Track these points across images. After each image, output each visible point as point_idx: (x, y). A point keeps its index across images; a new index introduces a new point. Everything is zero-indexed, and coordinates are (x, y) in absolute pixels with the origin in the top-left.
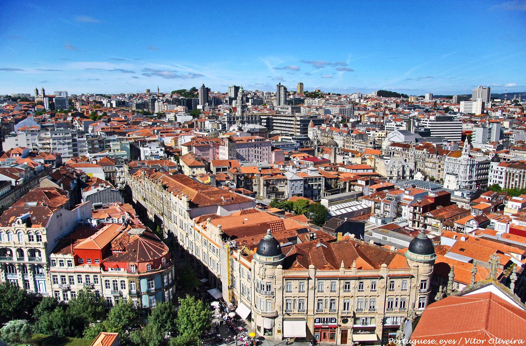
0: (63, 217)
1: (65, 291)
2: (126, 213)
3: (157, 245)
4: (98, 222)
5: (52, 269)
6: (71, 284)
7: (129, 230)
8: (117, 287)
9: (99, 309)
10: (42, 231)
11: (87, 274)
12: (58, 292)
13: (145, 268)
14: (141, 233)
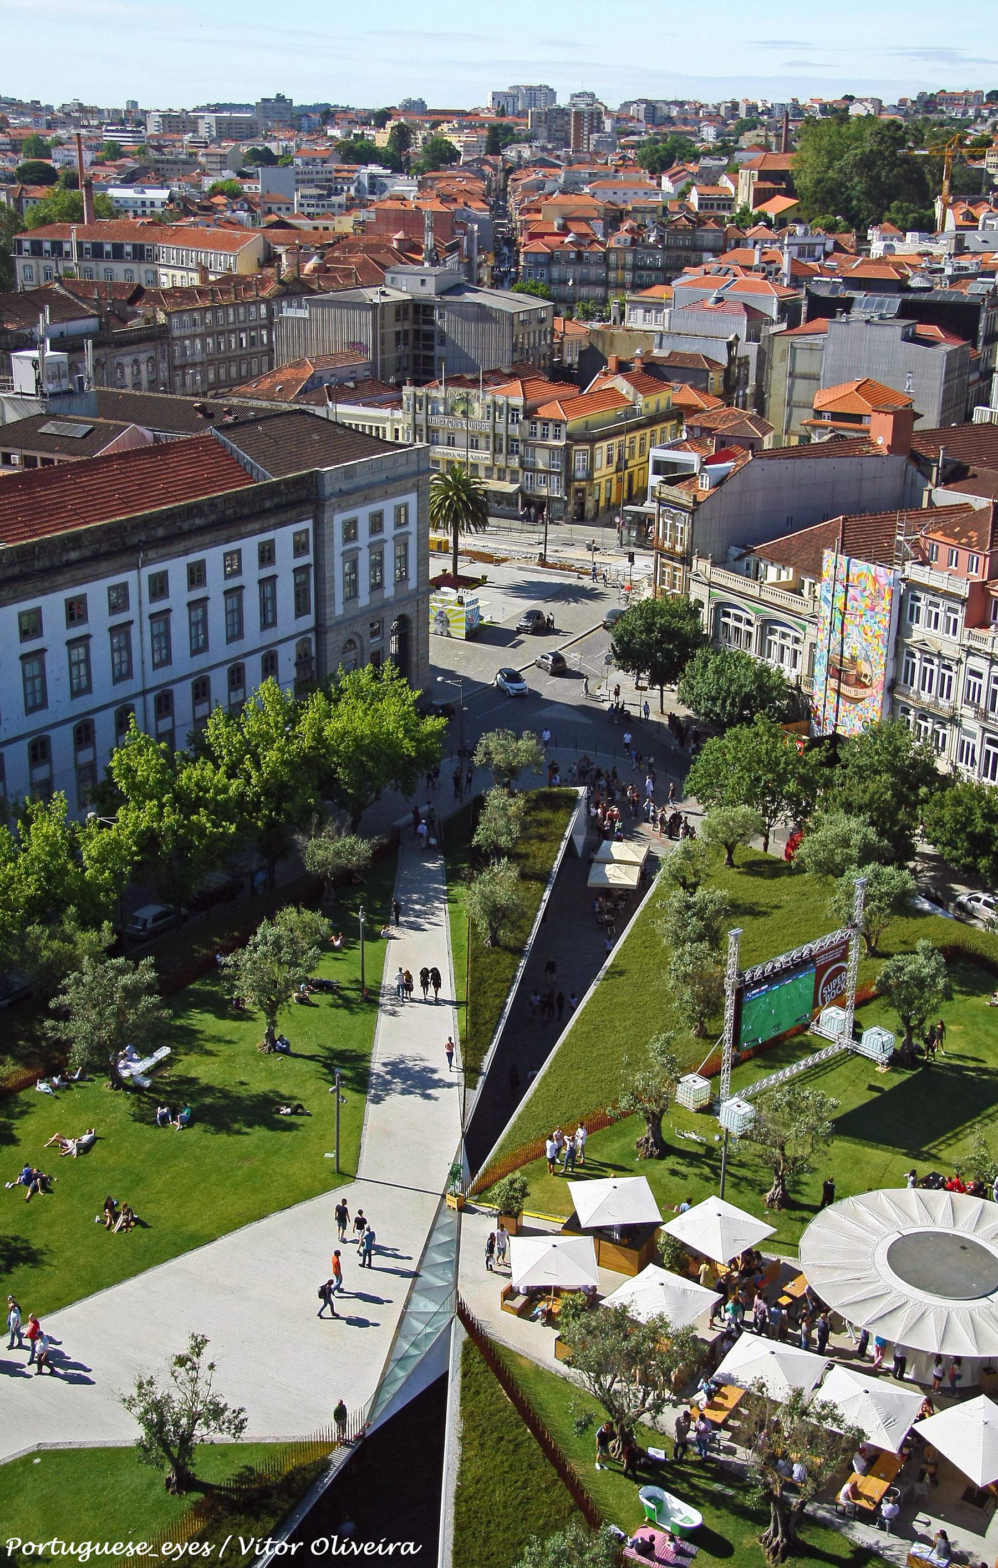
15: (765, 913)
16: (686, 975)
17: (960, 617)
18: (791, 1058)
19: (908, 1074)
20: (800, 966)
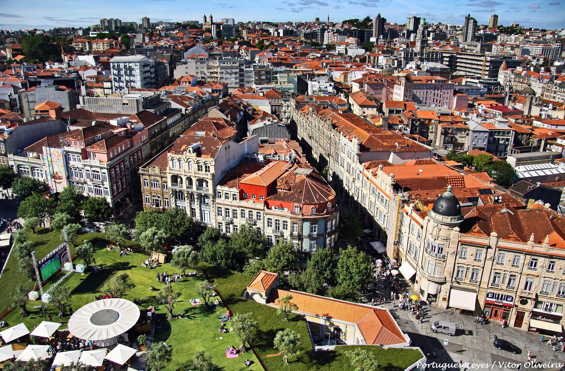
0: (231, 149)
2: (293, 151)
3: (323, 188)
4: (265, 158)
5: (218, 200)
7: (295, 169)
9: (260, 246)
10: (211, 161)
11: (250, 210)
13: (309, 210)
14: (308, 173)
15: (46, 243)
16: (24, 266)
17: (81, 157)
18: (59, 278)
19: (90, 273)
20: (53, 256)
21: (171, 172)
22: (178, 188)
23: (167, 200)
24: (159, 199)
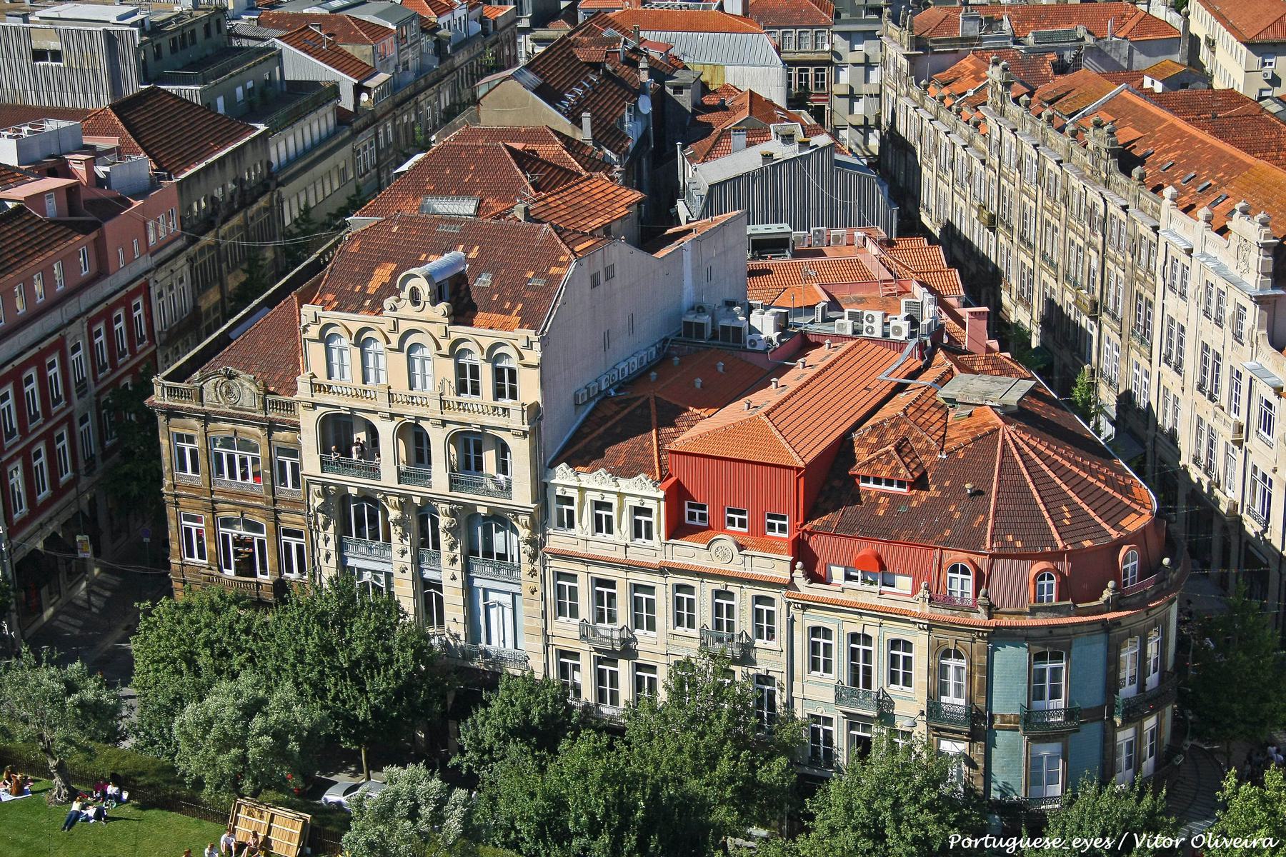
0: (617, 282)
1: (607, 657)
2: (920, 293)
3: (1092, 473)
4: (783, 325)
5: (557, 540)
6: (638, 624)
7: (942, 381)
8: (868, 671)
9: (774, 771)
10: (521, 346)
11: (719, 585)
12: (576, 655)
13: (1024, 587)
14: (1013, 398)
21: (320, 397)
22: (354, 483)
23: (294, 542)
24: (257, 536)
